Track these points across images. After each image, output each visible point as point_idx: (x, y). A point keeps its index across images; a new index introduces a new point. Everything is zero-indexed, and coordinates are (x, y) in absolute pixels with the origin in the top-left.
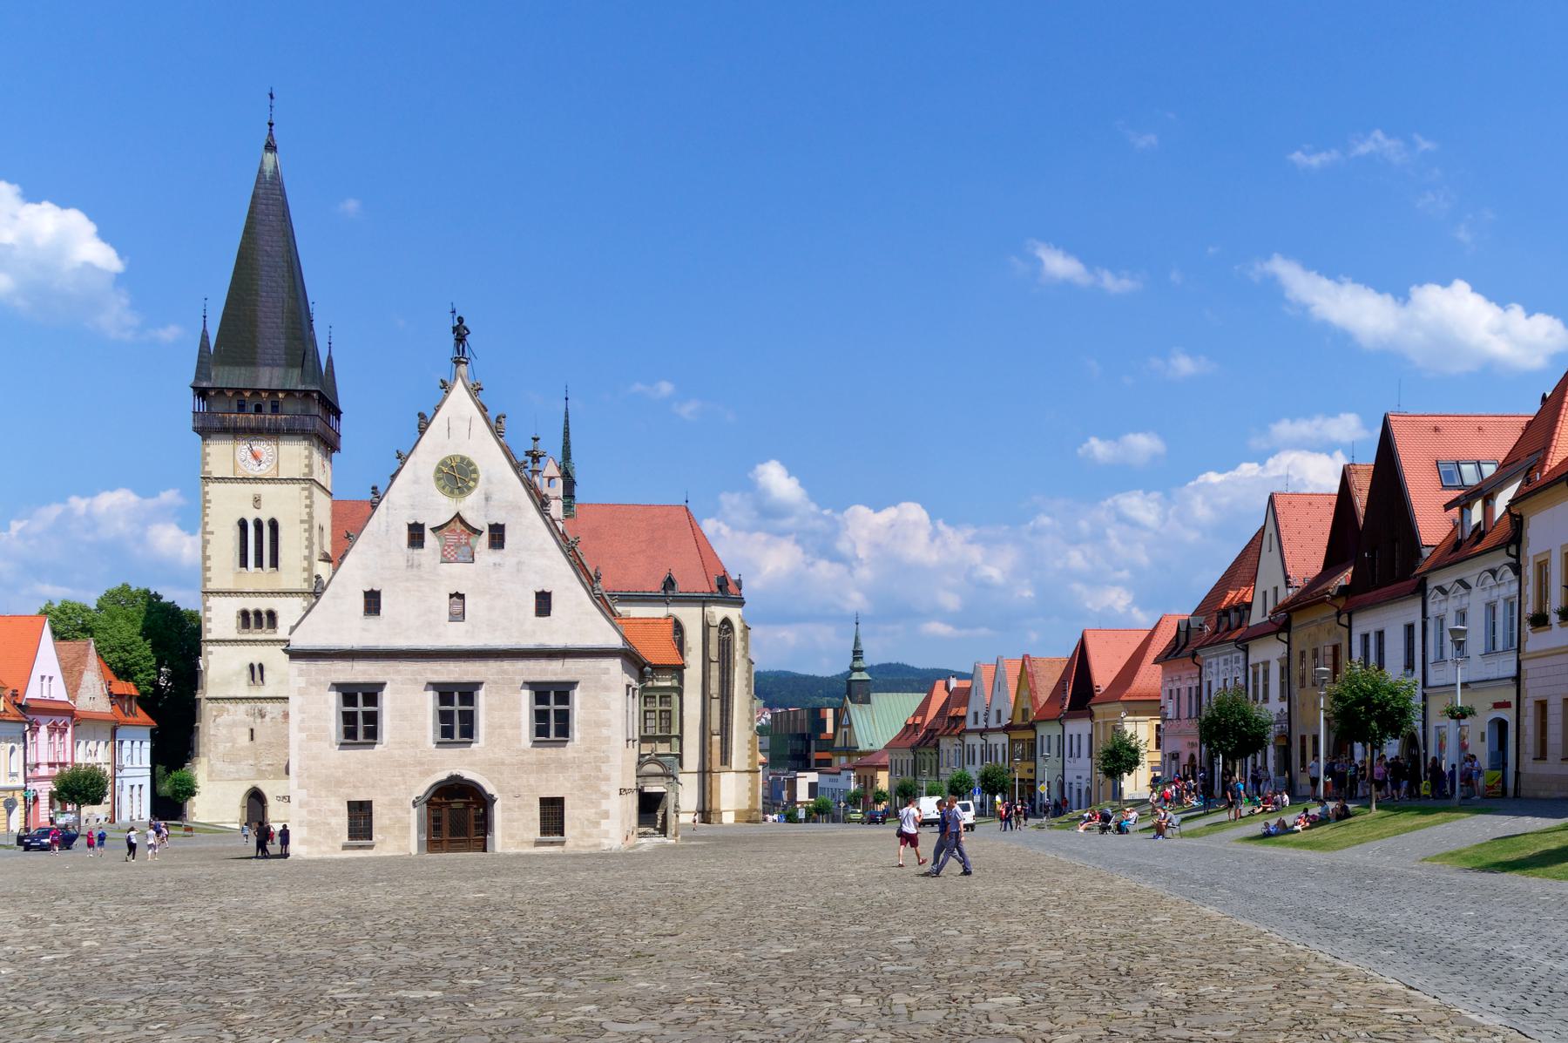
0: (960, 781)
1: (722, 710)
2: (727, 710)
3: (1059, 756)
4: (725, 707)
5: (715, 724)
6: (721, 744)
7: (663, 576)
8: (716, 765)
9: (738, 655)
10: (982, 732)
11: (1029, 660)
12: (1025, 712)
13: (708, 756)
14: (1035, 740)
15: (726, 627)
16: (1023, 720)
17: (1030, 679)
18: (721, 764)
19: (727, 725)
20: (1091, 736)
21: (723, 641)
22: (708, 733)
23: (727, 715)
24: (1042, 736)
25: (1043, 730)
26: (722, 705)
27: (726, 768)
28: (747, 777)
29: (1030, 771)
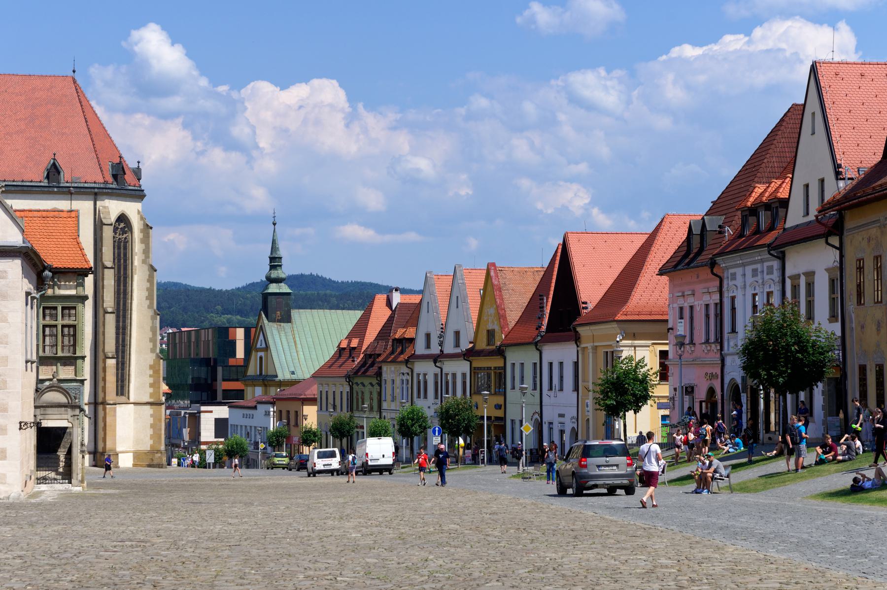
0: (413, 420)
1: (117, 328)
2: (124, 328)
3: (535, 389)
4: (121, 324)
5: (110, 345)
6: (117, 369)
7: (45, 162)
8: (111, 394)
9: (137, 261)
10: (436, 359)
11: (495, 269)
12: (491, 334)
13: (101, 384)
14: (504, 368)
15: (122, 225)
16: (488, 344)
17: (497, 293)
18: (117, 394)
19: (124, 346)
20: (576, 364)
21: (119, 242)
22: (101, 356)
23: (124, 334)
24: (514, 364)
25: (514, 356)
26: (118, 321)
27: (123, 399)
28: (148, 410)
29: (498, 407)
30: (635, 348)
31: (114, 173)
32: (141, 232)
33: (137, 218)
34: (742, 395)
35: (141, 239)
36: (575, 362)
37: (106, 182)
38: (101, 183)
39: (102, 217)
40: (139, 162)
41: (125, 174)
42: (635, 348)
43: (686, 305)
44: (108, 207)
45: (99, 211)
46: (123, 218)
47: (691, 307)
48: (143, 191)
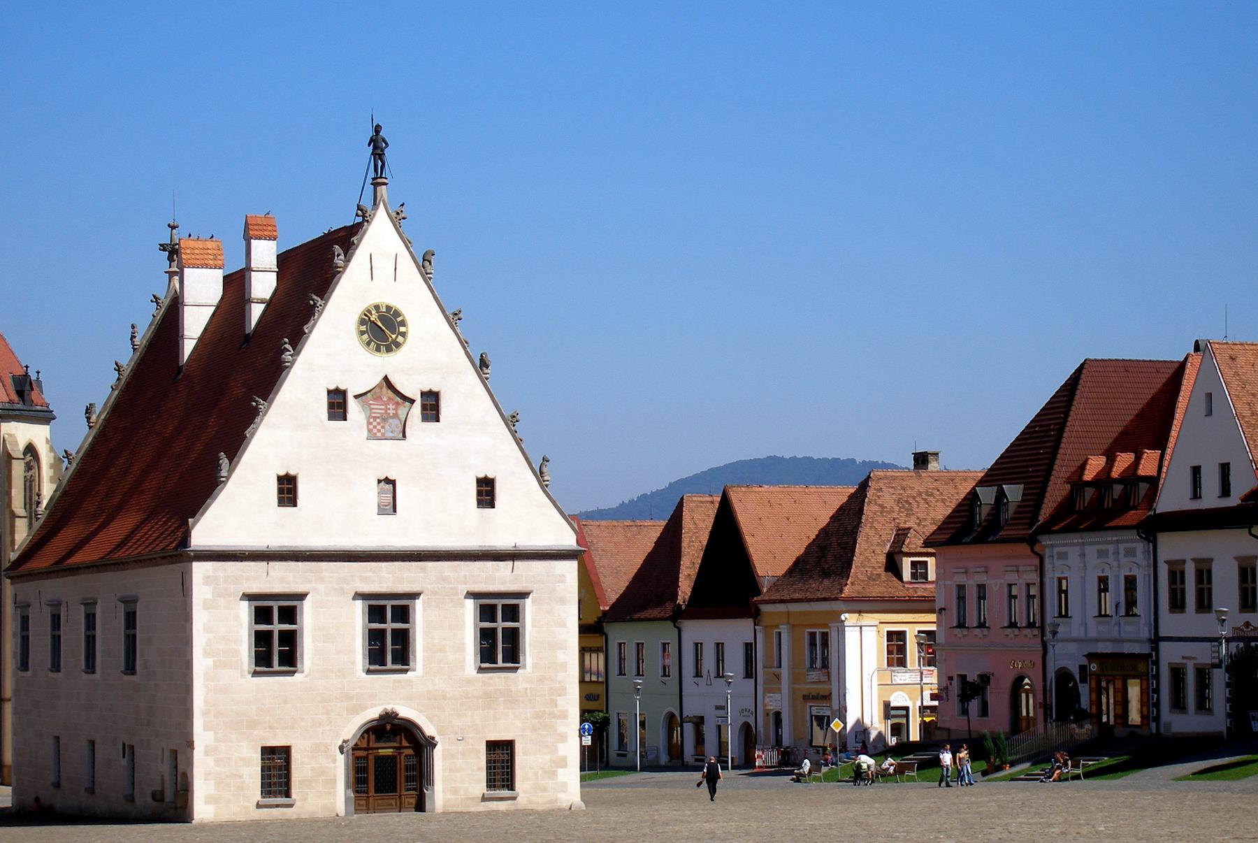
30: (861, 628)
31: (20, 389)
32: (51, 468)
33: (45, 449)
34: (1080, 685)
35: (51, 477)
36: (747, 644)
37: (11, 402)
38: (5, 403)
39: (9, 449)
40: (38, 372)
41: (32, 389)
42: (861, 627)
43: (971, 584)
44: (14, 434)
45: (4, 440)
46: (31, 449)
47: (981, 588)
48: (52, 412)
